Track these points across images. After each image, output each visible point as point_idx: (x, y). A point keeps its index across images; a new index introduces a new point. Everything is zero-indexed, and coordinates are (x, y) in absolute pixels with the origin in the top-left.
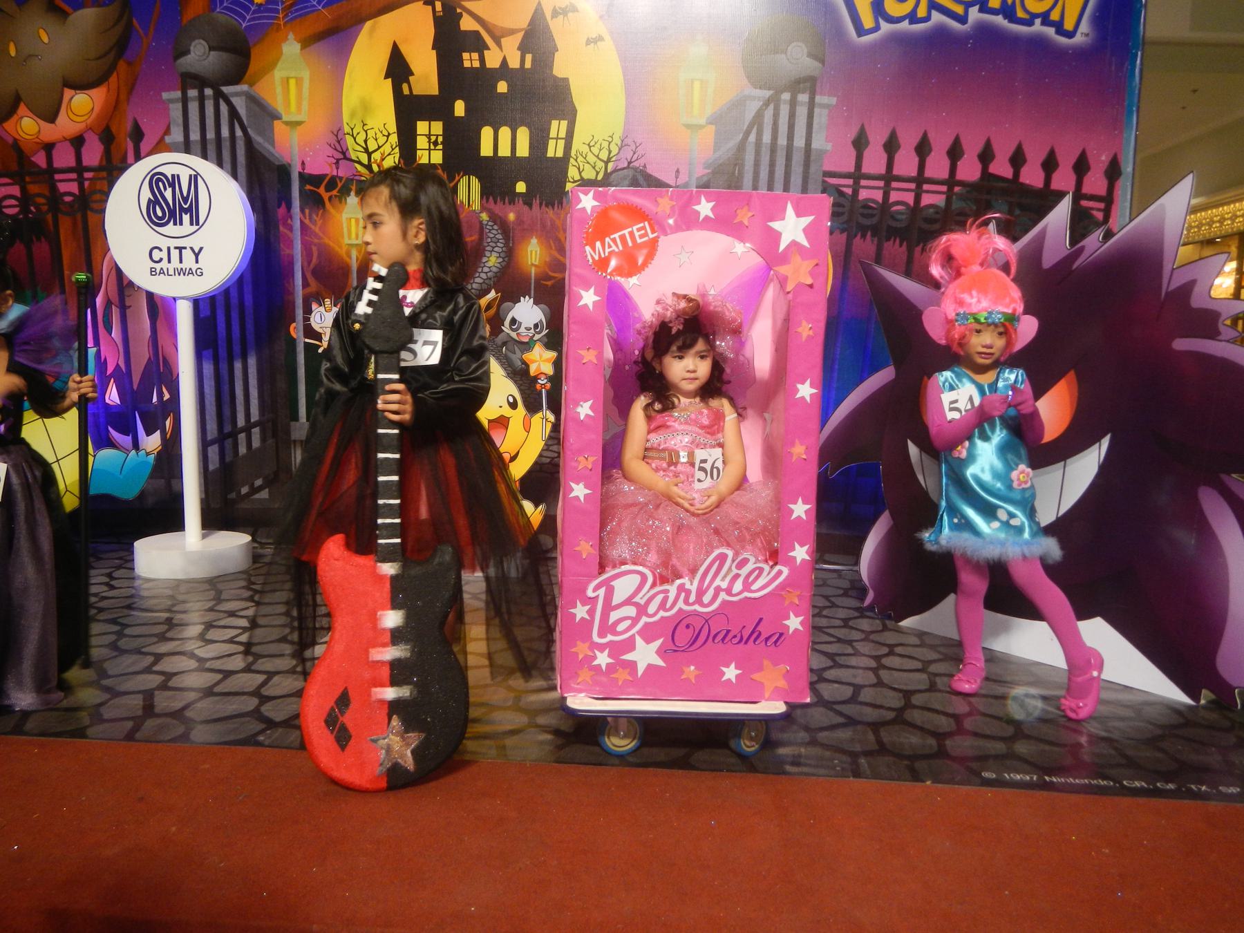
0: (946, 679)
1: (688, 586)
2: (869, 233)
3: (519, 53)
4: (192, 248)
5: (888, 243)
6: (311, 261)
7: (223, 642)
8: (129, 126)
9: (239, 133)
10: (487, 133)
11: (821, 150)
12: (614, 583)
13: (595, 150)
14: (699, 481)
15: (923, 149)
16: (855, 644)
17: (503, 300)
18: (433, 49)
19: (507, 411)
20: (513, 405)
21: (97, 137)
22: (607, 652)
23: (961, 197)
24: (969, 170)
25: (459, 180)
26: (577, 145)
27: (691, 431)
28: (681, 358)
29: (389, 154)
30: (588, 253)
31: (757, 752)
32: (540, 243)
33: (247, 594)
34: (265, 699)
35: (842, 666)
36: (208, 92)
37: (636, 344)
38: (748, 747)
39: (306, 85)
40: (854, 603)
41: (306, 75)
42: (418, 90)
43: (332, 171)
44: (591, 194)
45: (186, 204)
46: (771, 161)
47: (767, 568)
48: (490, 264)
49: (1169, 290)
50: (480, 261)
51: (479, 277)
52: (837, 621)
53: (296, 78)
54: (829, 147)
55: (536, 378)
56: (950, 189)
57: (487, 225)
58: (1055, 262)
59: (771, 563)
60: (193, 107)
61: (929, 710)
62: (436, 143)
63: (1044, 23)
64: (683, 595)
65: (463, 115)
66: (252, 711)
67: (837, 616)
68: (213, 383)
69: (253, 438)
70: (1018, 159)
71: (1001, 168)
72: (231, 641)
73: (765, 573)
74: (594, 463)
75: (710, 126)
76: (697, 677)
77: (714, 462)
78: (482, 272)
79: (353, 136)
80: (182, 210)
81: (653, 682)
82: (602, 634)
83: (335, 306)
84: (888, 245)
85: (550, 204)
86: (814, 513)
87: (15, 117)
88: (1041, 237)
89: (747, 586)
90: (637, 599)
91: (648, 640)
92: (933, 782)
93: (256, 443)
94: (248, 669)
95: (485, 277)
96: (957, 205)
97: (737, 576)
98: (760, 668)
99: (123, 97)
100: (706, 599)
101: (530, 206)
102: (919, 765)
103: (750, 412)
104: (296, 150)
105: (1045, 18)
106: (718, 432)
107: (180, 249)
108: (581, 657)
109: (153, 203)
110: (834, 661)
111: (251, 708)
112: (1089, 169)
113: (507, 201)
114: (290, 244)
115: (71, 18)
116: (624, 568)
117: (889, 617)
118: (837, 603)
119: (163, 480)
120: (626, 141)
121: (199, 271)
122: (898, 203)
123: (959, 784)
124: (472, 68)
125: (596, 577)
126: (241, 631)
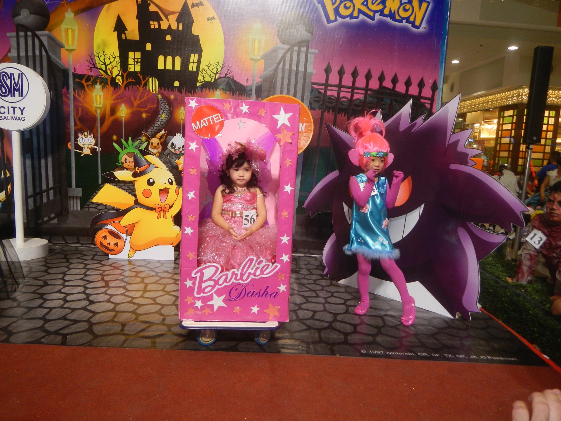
0: (353, 308)
1: (236, 272)
2: (331, 110)
3: (176, 23)
4: (19, 108)
6: (78, 114)
7: (31, 293)
9: (44, 53)
10: (161, 59)
11: (311, 73)
12: (204, 271)
14: (245, 224)
15: (355, 74)
16: (317, 292)
17: (168, 135)
18: (137, 19)
19: (168, 186)
20: (171, 183)
22: (200, 301)
23: (370, 96)
24: (374, 84)
25: (148, 79)
26: (202, 66)
27: (242, 203)
28: (237, 170)
29: (116, 66)
30: (193, 126)
31: (267, 343)
33: (44, 268)
34: (46, 321)
36: (29, 33)
37: (220, 163)
38: (263, 341)
40: (320, 272)
41: (76, 28)
42: (129, 38)
43: (88, 73)
44: (195, 100)
45: (17, 87)
46: (289, 76)
47: (271, 264)
48: (162, 118)
49: (450, 142)
51: (157, 124)
52: (311, 281)
53: (71, 29)
54: (314, 71)
56: (366, 92)
57: (161, 100)
58: (407, 126)
59: (273, 261)
60: (22, 41)
62: (137, 62)
63: (407, 22)
64: (234, 276)
65: (150, 49)
66: (40, 327)
67: (312, 279)
68: (31, 169)
69: (50, 195)
70: (395, 81)
71: (388, 84)
72: (34, 292)
73: (270, 267)
74: (195, 219)
75: (262, 60)
76: (240, 311)
77: (252, 217)
78: (158, 121)
79: (98, 57)
80: (15, 90)
81: (222, 314)
82: (198, 293)
83: (90, 135)
86: (291, 241)
88: (400, 117)
89: (262, 272)
90: (214, 278)
91: (219, 296)
92: (339, 355)
93: (51, 197)
94: (40, 306)
95: (160, 124)
96: (369, 99)
97: (258, 268)
98: (267, 307)
100: (244, 278)
101: (181, 92)
102: (336, 348)
103: (270, 193)
106: (254, 203)
107: (14, 108)
108: (189, 303)
110: (307, 300)
111: (39, 325)
112: (424, 86)
113: (170, 89)
114: (68, 106)
116: (209, 264)
117: (334, 279)
118: (313, 272)
119: (6, 214)
120: (224, 65)
121: (23, 118)
122: (344, 97)
123: (349, 356)
124: (155, 29)
125: (196, 268)
126: (39, 287)
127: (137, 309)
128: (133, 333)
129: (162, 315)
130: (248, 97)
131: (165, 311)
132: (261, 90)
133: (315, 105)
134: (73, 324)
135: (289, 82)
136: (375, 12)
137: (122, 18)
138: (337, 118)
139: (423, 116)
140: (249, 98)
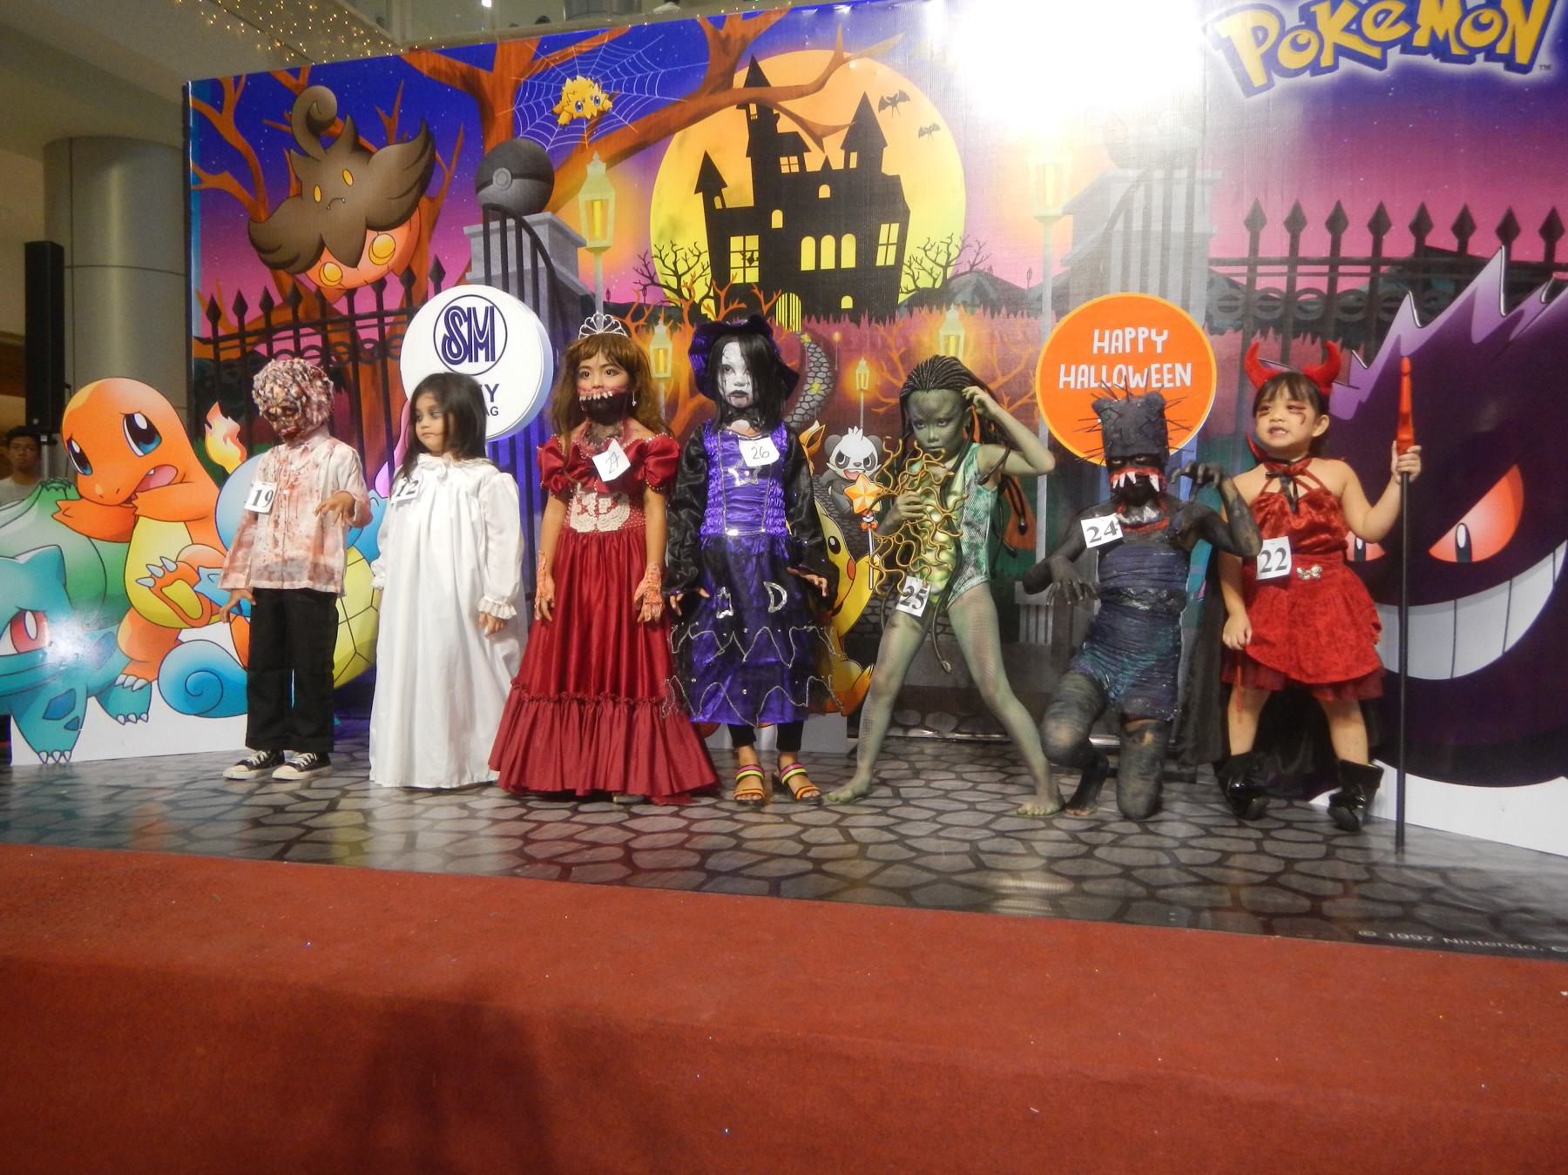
2: (1271, 331)
3: (843, 152)
4: (487, 386)
5: (1297, 340)
8: (429, 265)
9: (541, 264)
10: (808, 244)
13: (932, 254)
15: (1336, 223)
17: (828, 433)
21: (398, 278)
23: (1390, 278)
24: (1399, 245)
26: (910, 250)
29: (701, 276)
32: (870, 363)
35: (1216, 836)
36: (511, 222)
39: (612, 207)
41: (611, 196)
45: (481, 338)
48: (813, 392)
50: (802, 390)
53: (601, 200)
55: (860, 516)
56: (1375, 269)
60: (495, 240)
61: (1317, 877)
62: (751, 260)
63: (1487, 59)
70: (1463, 227)
71: (1442, 238)
79: (661, 258)
80: (481, 346)
84: (1296, 343)
85: (881, 319)
87: (319, 264)
88: (1469, 307)
96: (1384, 289)
99: (425, 234)
101: (858, 323)
102: (1276, 922)
104: (600, 278)
105: (1490, 52)
109: (448, 340)
115: (374, 157)
121: (494, 410)
122: (1307, 291)
124: (791, 173)
127: (741, 829)
128: (729, 869)
129: (802, 842)
130: (1032, 318)
131: (809, 836)
132: (1067, 295)
133: (1220, 320)
134: (589, 849)
135: (1145, 264)
136: (1386, 46)
137: (715, 159)
138: (1292, 352)
139: (1541, 289)
140: (1036, 318)
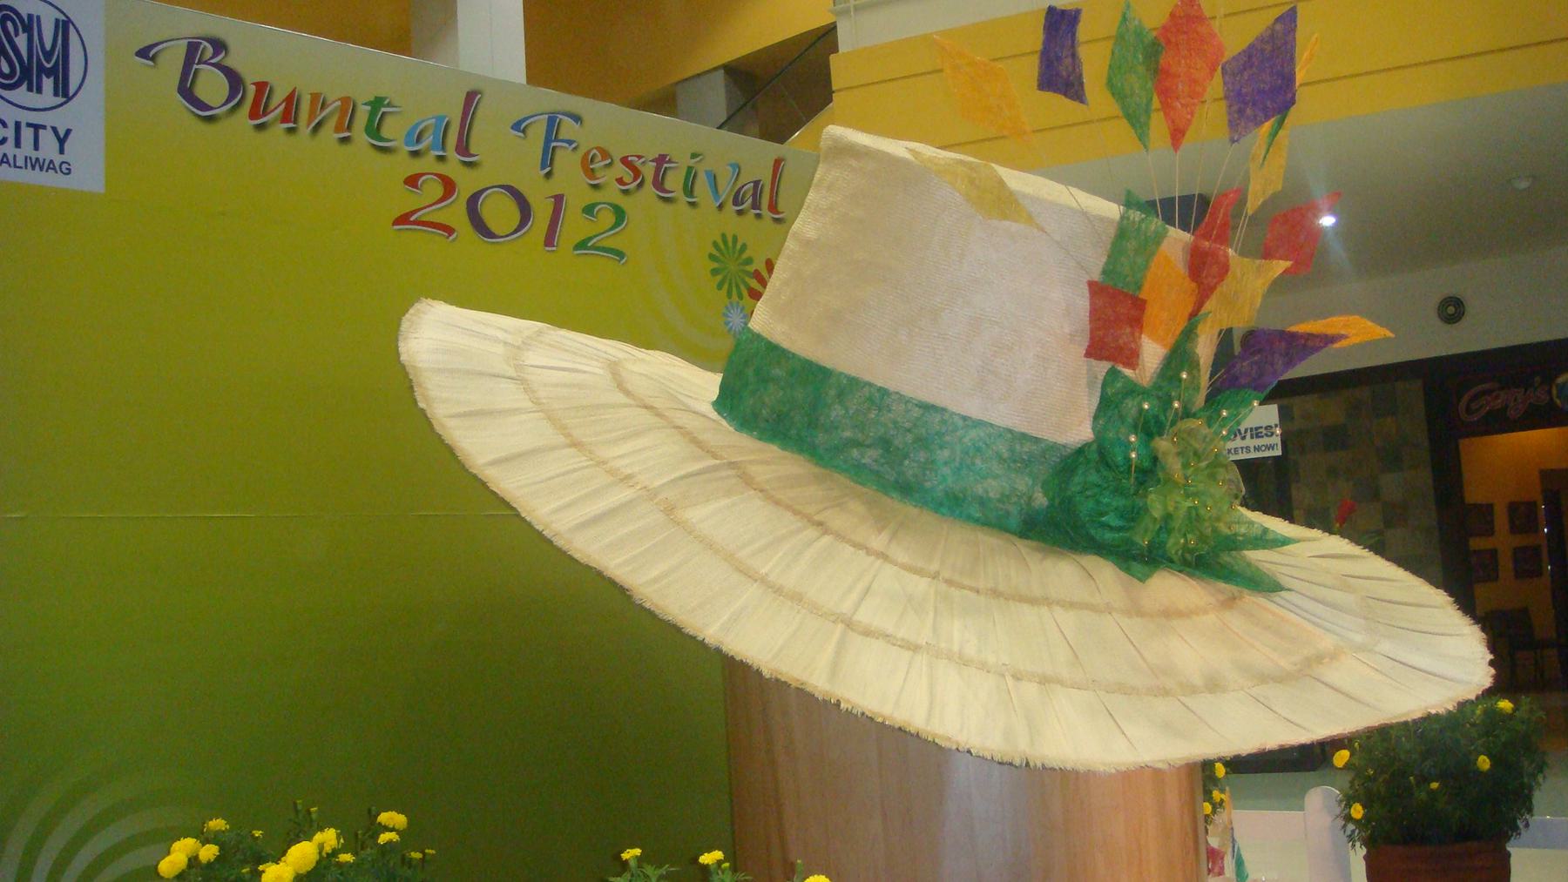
4: (54, 129)
107: (37, 128)
121: (64, 166)
